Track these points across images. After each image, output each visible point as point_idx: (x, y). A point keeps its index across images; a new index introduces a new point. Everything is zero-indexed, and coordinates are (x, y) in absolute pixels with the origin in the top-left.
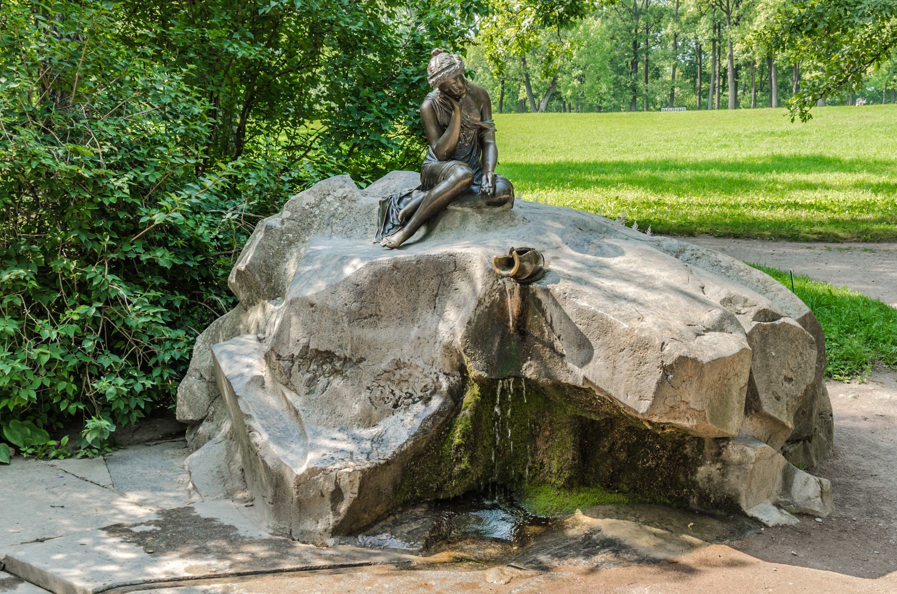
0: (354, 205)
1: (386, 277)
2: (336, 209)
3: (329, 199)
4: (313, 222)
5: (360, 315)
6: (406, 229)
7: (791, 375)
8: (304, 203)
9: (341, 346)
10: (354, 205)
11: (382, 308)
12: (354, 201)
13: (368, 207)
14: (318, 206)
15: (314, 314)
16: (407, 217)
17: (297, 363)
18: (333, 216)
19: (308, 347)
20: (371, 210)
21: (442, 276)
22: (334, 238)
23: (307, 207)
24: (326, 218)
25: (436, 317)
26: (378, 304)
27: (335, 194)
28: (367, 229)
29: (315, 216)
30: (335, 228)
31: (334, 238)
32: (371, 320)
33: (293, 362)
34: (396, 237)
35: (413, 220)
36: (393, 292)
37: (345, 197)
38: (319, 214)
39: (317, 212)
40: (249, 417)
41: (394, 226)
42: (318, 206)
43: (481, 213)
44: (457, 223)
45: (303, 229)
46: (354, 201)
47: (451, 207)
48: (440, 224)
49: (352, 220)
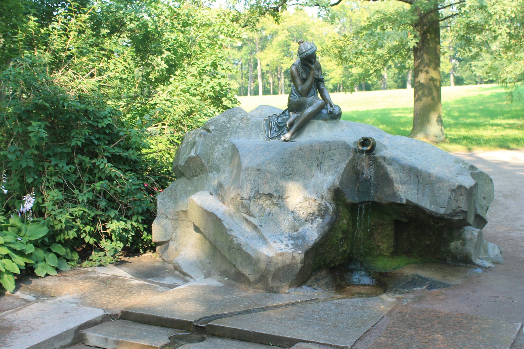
0: (248, 122)
1: (296, 154)
2: (239, 124)
3: (234, 119)
4: (227, 131)
5: (285, 174)
6: (292, 131)
7: (485, 196)
8: (221, 121)
9: (276, 191)
10: (248, 122)
11: (295, 170)
12: (248, 120)
13: (257, 123)
14: (229, 123)
15: (260, 175)
16: (291, 125)
17: (252, 201)
18: (238, 128)
19: (258, 192)
21: (323, 153)
23: (223, 124)
24: (235, 129)
25: (322, 174)
26: (293, 169)
27: (237, 116)
28: (258, 134)
29: (228, 128)
31: (241, 139)
32: (290, 176)
33: (250, 200)
34: (288, 135)
35: (295, 127)
36: (300, 162)
37: (243, 118)
38: (230, 127)
39: (229, 126)
40: (232, 230)
41: (276, 131)
42: (229, 123)
44: (316, 128)
45: (223, 135)
46: (248, 120)
49: (249, 129)
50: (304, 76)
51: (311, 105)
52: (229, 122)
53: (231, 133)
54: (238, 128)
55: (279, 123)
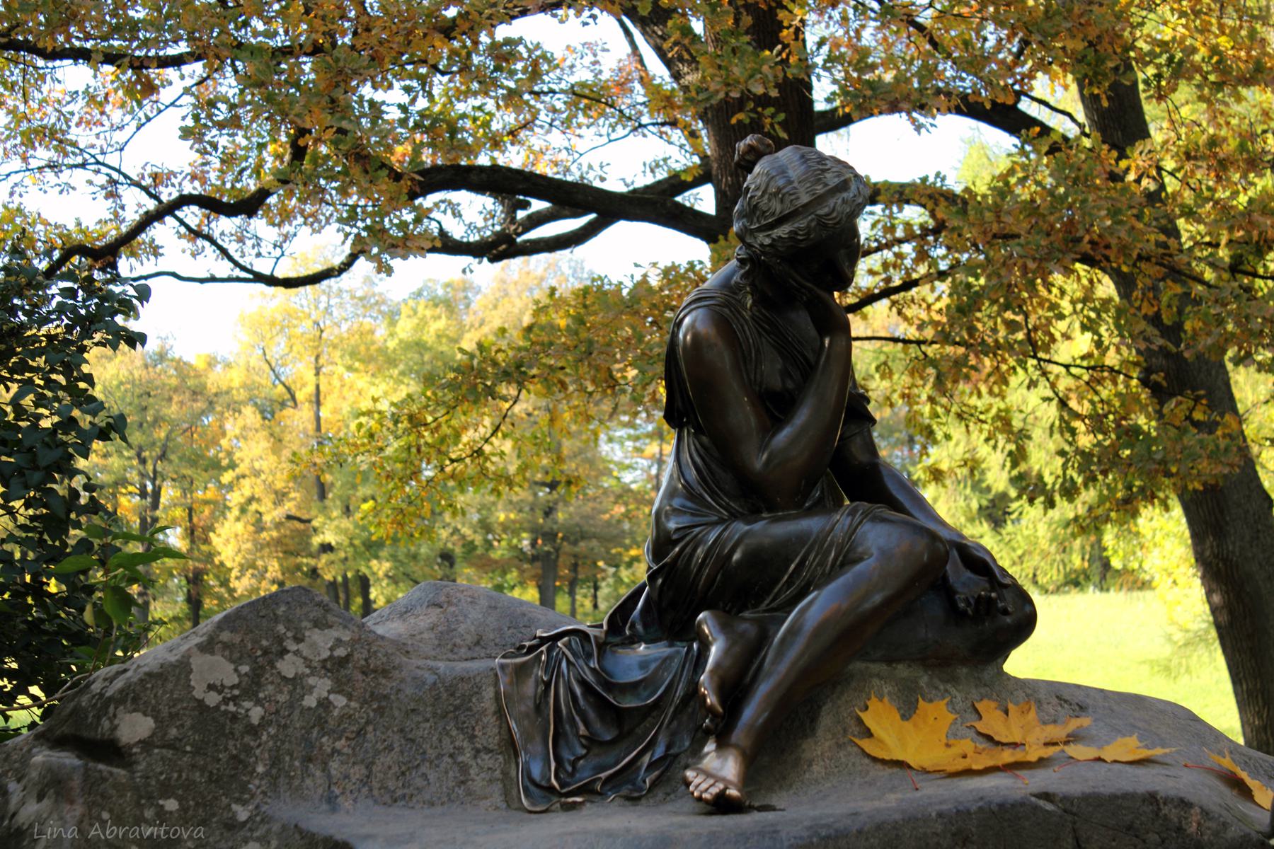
2: (325, 704)
3: (288, 666)
10: (386, 686)
12: (385, 673)
20: (467, 698)
22: (346, 803)
23: (212, 699)
28: (464, 769)
29: (254, 731)
30: (334, 766)
38: (264, 723)
39: (256, 714)
43: (954, 680)
46: (385, 673)
47: (858, 666)
48: (826, 720)
49: (397, 740)
50: (772, 371)
51: (848, 559)
52: (251, 688)
53: (275, 761)
54: (321, 722)
55: (610, 686)
